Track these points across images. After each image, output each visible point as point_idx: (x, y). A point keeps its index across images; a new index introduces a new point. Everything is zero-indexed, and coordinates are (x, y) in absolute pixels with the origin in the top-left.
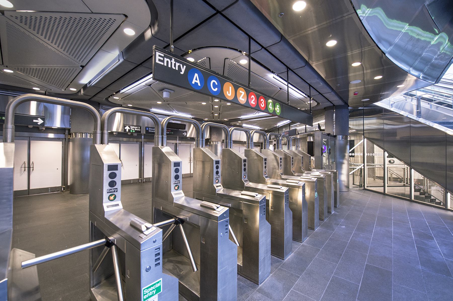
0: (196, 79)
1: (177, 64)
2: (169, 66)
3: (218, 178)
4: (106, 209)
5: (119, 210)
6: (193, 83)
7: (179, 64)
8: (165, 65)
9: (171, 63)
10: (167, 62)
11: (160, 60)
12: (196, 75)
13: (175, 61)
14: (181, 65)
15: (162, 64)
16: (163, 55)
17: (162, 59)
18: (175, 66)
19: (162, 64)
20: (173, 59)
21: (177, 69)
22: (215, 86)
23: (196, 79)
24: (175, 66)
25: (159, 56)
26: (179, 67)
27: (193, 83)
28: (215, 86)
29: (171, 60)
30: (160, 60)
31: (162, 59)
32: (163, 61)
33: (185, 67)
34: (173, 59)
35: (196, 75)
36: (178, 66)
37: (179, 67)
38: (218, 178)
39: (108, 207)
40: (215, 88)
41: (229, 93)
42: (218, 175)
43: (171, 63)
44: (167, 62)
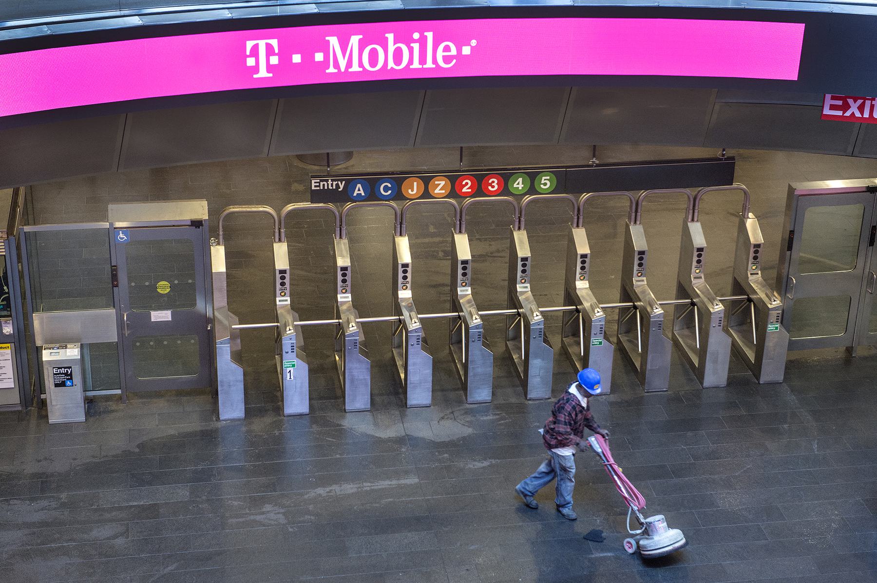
0: (359, 190)
1: (335, 183)
2: (326, 188)
3: (407, 285)
4: (278, 303)
5: (287, 305)
6: (355, 194)
7: (337, 182)
8: (322, 188)
9: (328, 184)
10: (324, 185)
11: (315, 186)
12: (359, 186)
13: (332, 180)
14: (339, 182)
15: (319, 188)
16: (319, 181)
17: (318, 184)
18: (332, 185)
19: (319, 188)
20: (330, 180)
21: (334, 188)
22: (386, 189)
23: (359, 190)
24: (332, 185)
25: (315, 183)
26: (337, 185)
27: (355, 194)
28: (386, 189)
29: (327, 181)
30: (315, 186)
31: (318, 184)
32: (319, 186)
33: (344, 182)
34: (330, 180)
35: (359, 186)
36: (336, 184)
37: (337, 185)
38: (407, 285)
39: (280, 301)
40: (386, 191)
41: (412, 191)
42: (407, 280)
43: (328, 184)
44: (324, 185)
